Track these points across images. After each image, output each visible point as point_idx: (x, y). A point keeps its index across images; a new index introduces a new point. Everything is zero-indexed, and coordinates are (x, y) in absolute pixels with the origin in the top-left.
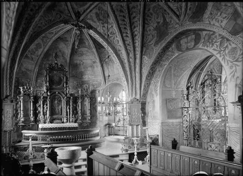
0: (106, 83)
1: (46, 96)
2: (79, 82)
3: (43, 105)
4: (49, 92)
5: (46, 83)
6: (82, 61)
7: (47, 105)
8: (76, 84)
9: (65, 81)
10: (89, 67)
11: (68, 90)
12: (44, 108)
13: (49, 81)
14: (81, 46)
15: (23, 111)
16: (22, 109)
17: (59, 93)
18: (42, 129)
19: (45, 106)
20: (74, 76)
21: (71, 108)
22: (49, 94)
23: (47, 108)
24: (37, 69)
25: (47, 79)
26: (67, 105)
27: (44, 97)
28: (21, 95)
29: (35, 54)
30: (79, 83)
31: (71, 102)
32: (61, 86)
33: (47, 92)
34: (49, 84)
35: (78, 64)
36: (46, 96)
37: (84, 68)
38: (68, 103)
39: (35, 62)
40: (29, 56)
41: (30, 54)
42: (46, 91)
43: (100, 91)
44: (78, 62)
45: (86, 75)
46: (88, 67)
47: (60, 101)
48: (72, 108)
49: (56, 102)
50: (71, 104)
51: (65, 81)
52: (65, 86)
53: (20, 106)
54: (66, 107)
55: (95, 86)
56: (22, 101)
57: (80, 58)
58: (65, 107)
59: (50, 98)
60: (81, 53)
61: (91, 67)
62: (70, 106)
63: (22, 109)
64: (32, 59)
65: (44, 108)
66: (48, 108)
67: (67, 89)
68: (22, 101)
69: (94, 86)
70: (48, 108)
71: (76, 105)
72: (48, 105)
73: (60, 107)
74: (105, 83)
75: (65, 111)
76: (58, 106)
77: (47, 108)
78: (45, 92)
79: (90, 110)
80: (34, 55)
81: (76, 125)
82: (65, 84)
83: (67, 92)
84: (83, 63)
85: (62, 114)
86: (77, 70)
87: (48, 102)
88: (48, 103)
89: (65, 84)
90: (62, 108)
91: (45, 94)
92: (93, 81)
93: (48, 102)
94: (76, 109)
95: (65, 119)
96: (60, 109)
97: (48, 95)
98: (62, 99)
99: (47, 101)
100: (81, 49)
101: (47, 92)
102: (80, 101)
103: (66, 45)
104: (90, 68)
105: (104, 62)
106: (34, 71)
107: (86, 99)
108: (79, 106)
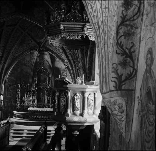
1: (35, 90)
3: (33, 96)
4: (37, 88)
7: (35, 96)
15: (20, 99)
16: (19, 98)
17: (43, 88)
18: (31, 111)
22: (36, 88)
26: (48, 96)
27: (33, 91)
28: (19, 89)
32: (45, 83)
33: (35, 87)
34: (37, 82)
38: (49, 95)
40: (27, 65)
41: (27, 63)
42: (34, 87)
47: (44, 93)
49: (42, 94)
53: (18, 96)
54: (48, 98)
56: (19, 93)
59: (37, 91)
63: (19, 98)
66: (36, 97)
67: (48, 85)
68: (19, 93)
70: (36, 97)
71: (55, 96)
72: (36, 96)
73: (44, 97)
81: (51, 109)
82: (47, 82)
85: (45, 102)
87: (36, 94)
89: (47, 82)
90: (45, 97)
93: (36, 94)
94: (55, 99)
97: (36, 89)
98: (46, 92)
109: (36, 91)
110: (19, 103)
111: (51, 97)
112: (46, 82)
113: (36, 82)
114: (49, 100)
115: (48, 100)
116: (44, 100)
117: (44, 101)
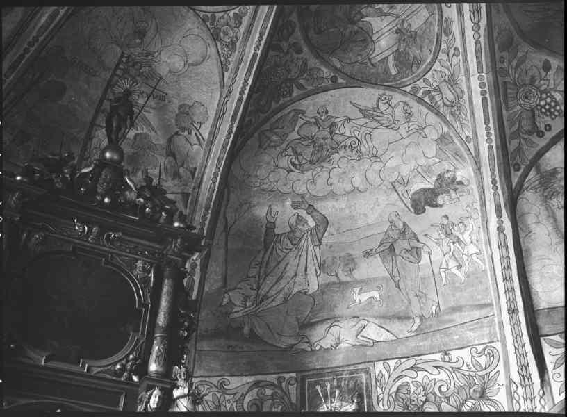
2: (273, 378)
6: (311, 209)
8: (248, 399)
9: (161, 319)
10: (368, 254)
14: (326, 73)
30: (269, 392)
35: (277, 231)
37: (322, 266)
44: (285, 213)
45: (333, 319)
46: (357, 253)
52: (153, 367)
57: (300, 182)
60: (313, 140)
61: (389, 250)
84: (324, 222)
86: (270, 281)
92: (411, 363)
100: (327, 96)
103: (215, 37)
104: (377, 261)
105: (532, 174)
112: (128, 354)
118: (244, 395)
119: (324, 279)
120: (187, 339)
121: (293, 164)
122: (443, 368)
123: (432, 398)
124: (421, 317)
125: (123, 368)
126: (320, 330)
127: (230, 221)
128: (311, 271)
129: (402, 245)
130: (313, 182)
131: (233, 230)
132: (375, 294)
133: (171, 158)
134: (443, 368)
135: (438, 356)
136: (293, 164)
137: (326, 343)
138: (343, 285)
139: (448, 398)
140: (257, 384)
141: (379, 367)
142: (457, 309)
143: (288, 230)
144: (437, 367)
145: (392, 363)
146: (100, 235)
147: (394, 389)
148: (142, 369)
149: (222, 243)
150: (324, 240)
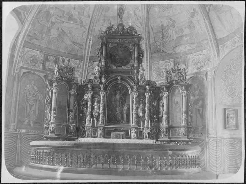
0: (220, 55)
4: (105, 78)
5: (100, 61)
6: (171, 19)
7: (99, 102)
10: (186, 28)
11: (141, 72)
12: (93, 108)
13: (106, 59)
17: (121, 79)
19: (95, 104)
20: (160, 50)
21: (146, 109)
22: (103, 80)
23: (99, 107)
24: (90, 40)
25: (102, 53)
26: (138, 103)
29: (85, 13)
31: (147, 96)
36: (98, 83)
38: (140, 99)
39: (87, 28)
41: (77, 13)
43: (209, 74)
48: (150, 109)
49: (118, 97)
50: (146, 102)
51: (136, 56)
54: (137, 108)
55: (199, 65)
58: (134, 106)
59: (105, 88)
62: (144, 105)
64: (82, 22)
65: (93, 108)
66: (101, 109)
69: (197, 64)
70: (101, 109)
71: (158, 104)
72: (101, 102)
73: (125, 108)
74: (218, 55)
75: (134, 115)
76: (122, 105)
77: (99, 107)
78: (95, 78)
79: (186, 112)
80: (83, 15)
83: (139, 78)
85: (128, 121)
88: (101, 99)
90: (129, 109)
91: (96, 81)
95: (134, 131)
96: (125, 112)
97: (101, 83)
98: (130, 91)
99: (100, 95)
101: (100, 78)
102: (165, 94)
106: (86, 45)
107: (179, 91)
108: (163, 106)
109: (102, 86)
110: (52, 121)
111: (147, 105)
112: (131, 63)
113: (103, 64)
114: (141, 114)
115: (137, 114)
116: (125, 116)
117: (125, 120)
118: (163, 65)
119: (177, 35)
120: (142, 58)
121: (164, 10)
122: (201, 55)
123: (199, 62)
124: (197, 43)
125: (130, 67)
126: (177, 48)
127: (152, 26)
128: (174, 34)
129: (191, 25)
130: (169, 13)
131: (154, 28)
132: (188, 38)
133: (135, 16)
134: (201, 55)
135: (200, 52)
136: (164, 10)
137: (179, 51)
138: (182, 36)
139: (202, 61)
140: (165, 62)
141: (189, 55)
142: (202, 41)
143: (167, 25)
144: (200, 54)
145: (192, 54)
146: (122, 41)
147: (192, 60)
148: (133, 66)
149: (152, 32)
150: (176, 26)
